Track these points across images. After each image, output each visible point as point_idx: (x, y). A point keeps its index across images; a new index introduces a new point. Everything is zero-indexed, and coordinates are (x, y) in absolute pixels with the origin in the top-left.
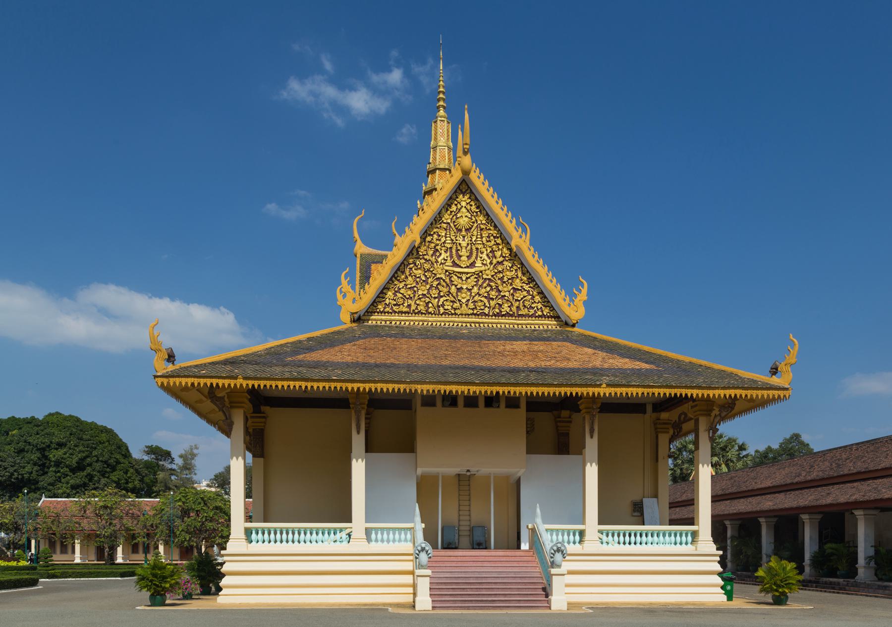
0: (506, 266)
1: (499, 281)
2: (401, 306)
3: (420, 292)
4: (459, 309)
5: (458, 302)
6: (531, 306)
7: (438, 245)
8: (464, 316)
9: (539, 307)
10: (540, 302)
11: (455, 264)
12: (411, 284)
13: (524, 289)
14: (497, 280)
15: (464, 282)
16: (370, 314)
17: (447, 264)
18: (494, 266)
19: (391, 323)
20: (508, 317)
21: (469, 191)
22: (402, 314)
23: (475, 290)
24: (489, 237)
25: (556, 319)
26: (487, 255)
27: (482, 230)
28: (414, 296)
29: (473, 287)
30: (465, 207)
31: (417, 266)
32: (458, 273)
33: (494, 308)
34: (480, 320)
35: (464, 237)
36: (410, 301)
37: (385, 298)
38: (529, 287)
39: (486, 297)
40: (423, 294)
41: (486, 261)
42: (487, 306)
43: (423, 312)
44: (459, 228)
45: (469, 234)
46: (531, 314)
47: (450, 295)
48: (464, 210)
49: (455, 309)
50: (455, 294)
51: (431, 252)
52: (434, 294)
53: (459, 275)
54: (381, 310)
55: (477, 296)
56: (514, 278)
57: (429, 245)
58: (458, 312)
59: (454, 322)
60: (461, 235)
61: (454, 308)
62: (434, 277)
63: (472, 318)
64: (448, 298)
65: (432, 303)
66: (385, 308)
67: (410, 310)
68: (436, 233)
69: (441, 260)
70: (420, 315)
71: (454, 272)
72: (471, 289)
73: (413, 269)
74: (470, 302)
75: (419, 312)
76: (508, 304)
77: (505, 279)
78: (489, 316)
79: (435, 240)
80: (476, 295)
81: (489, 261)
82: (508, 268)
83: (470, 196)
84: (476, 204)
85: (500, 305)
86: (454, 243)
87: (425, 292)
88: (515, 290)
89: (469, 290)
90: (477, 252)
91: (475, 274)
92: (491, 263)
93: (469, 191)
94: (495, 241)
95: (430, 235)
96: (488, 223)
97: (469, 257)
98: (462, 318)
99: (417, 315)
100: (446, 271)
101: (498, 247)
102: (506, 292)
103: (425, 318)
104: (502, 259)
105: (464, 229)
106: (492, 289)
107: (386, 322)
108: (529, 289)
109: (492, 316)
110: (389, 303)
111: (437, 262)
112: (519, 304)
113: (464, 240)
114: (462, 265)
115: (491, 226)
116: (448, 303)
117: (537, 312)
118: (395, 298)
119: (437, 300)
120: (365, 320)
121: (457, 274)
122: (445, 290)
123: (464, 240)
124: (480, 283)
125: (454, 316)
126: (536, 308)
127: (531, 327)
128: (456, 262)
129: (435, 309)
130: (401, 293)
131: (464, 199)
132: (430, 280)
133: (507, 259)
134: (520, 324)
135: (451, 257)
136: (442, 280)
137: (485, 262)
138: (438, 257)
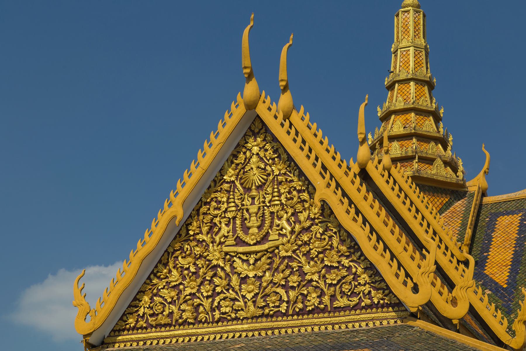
0: (316, 233)
1: (304, 258)
2: (160, 316)
3: (188, 291)
4: (242, 310)
5: (241, 300)
6: (353, 293)
7: (216, 217)
8: (250, 321)
9: (366, 292)
10: (368, 283)
11: (239, 242)
12: (176, 281)
13: (343, 265)
14: (301, 256)
15: (251, 267)
16: (117, 333)
17: (227, 243)
18: (297, 237)
19: (145, 344)
20: (318, 313)
21: (263, 131)
22: (161, 328)
25: (396, 308)
26: (288, 220)
27: (280, 183)
28: (178, 299)
30: (258, 154)
31: (185, 253)
32: (243, 254)
33: (295, 302)
34: (275, 324)
35: (253, 199)
36: (173, 307)
37: (138, 306)
38: (350, 261)
39: (283, 286)
40: (190, 294)
41: (286, 229)
42: (284, 301)
43: (190, 321)
44: (247, 187)
45: (261, 193)
47: (230, 291)
48: (255, 159)
49: (237, 311)
50: (237, 288)
51: (205, 229)
52: (207, 292)
54: (132, 325)
55: (270, 286)
56: (327, 249)
57: (204, 219)
59: (235, 331)
60: (250, 197)
61: (235, 310)
62: (208, 266)
63: (262, 322)
64: (228, 294)
65: (202, 305)
66: (137, 321)
67: (172, 321)
68: (215, 199)
69: (220, 238)
70: (186, 327)
72: (261, 277)
73: (180, 258)
74: (260, 296)
75: (185, 321)
76: (316, 293)
77: (314, 253)
78: (288, 316)
80: (268, 285)
81: (289, 228)
82: (318, 235)
83: (266, 137)
84: (273, 147)
85: (305, 296)
86: (239, 210)
87: (194, 291)
89: (260, 278)
90: (273, 219)
91: (268, 252)
92: (292, 232)
93: (263, 131)
95: (206, 203)
96: (290, 172)
97: (260, 228)
98: (247, 323)
99: (182, 327)
100: (227, 254)
101: (304, 206)
103: (194, 331)
104: (308, 223)
105: (254, 187)
106: (292, 273)
107: (138, 343)
108: (351, 264)
109: (292, 315)
110: (144, 314)
112: (335, 291)
113: (253, 204)
115: (294, 175)
116: (227, 303)
117: (363, 301)
118: (151, 305)
120: (109, 344)
121: (241, 256)
122: (224, 282)
123: (253, 204)
124: (275, 266)
125: (235, 322)
126: (361, 294)
127: (360, 326)
128: (241, 237)
129: (208, 314)
130: (161, 297)
131: (255, 143)
133: (316, 221)
134: (337, 324)
135: (234, 231)
136: (219, 269)
138: (216, 235)
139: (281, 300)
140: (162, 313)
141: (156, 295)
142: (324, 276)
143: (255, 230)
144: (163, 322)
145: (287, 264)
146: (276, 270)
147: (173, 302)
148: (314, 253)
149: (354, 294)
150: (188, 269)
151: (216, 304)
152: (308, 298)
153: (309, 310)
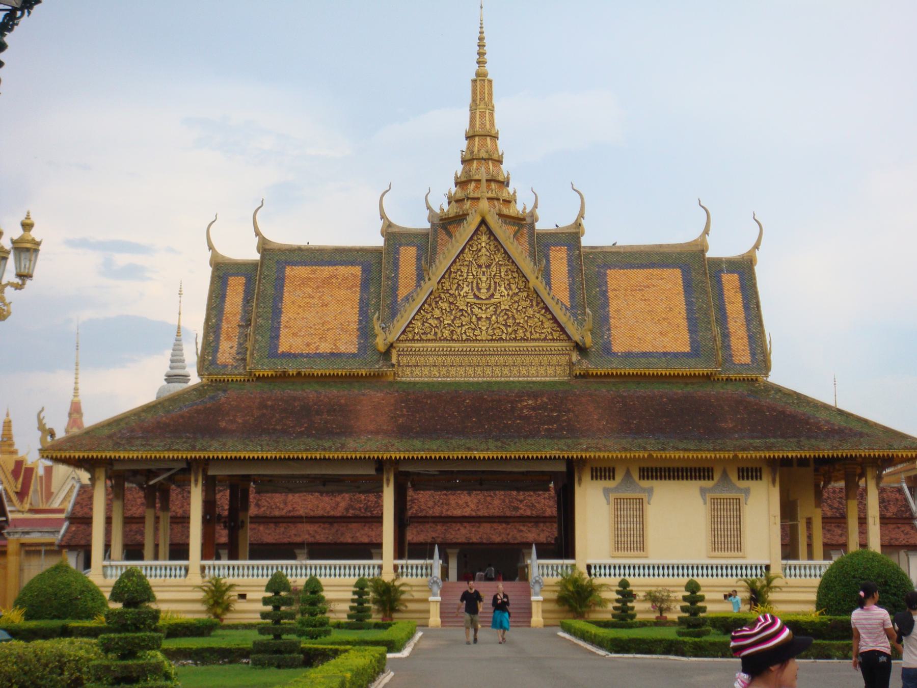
2: (429, 335)
3: (446, 322)
17: (468, 297)
24: (507, 272)
26: (505, 288)
27: (501, 265)
28: (440, 325)
29: (491, 316)
32: (478, 304)
33: (511, 334)
40: (448, 324)
46: (542, 338)
48: (484, 250)
49: (476, 336)
51: (455, 287)
53: (479, 306)
58: (479, 338)
66: (414, 336)
71: (475, 304)
73: (440, 303)
74: (490, 329)
79: (458, 276)
80: (495, 323)
81: (506, 293)
82: (524, 298)
84: (494, 244)
85: (516, 331)
87: (450, 322)
88: (529, 317)
92: (508, 295)
93: (488, 232)
94: (512, 275)
97: (489, 289)
100: (468, 303)
104: (517, 290)
105: (484, 266)
106: (508, 318)
111: (460, 295)
113: (484, 274)
114: (482, 297)
119: (460, 329)
124: (498, 313)
125: (475, 342)
132: (454, 312)
135: (472, 290)
137: (503, 294)
138: (461, 290)
139: (503, 332)
140: (430, 333)
141: (426, 322)
142: (527, 321)
143: (486, 291)
146: (499, 315)
147: (437, 327)
148: (520, 308)
150: (446, 310)
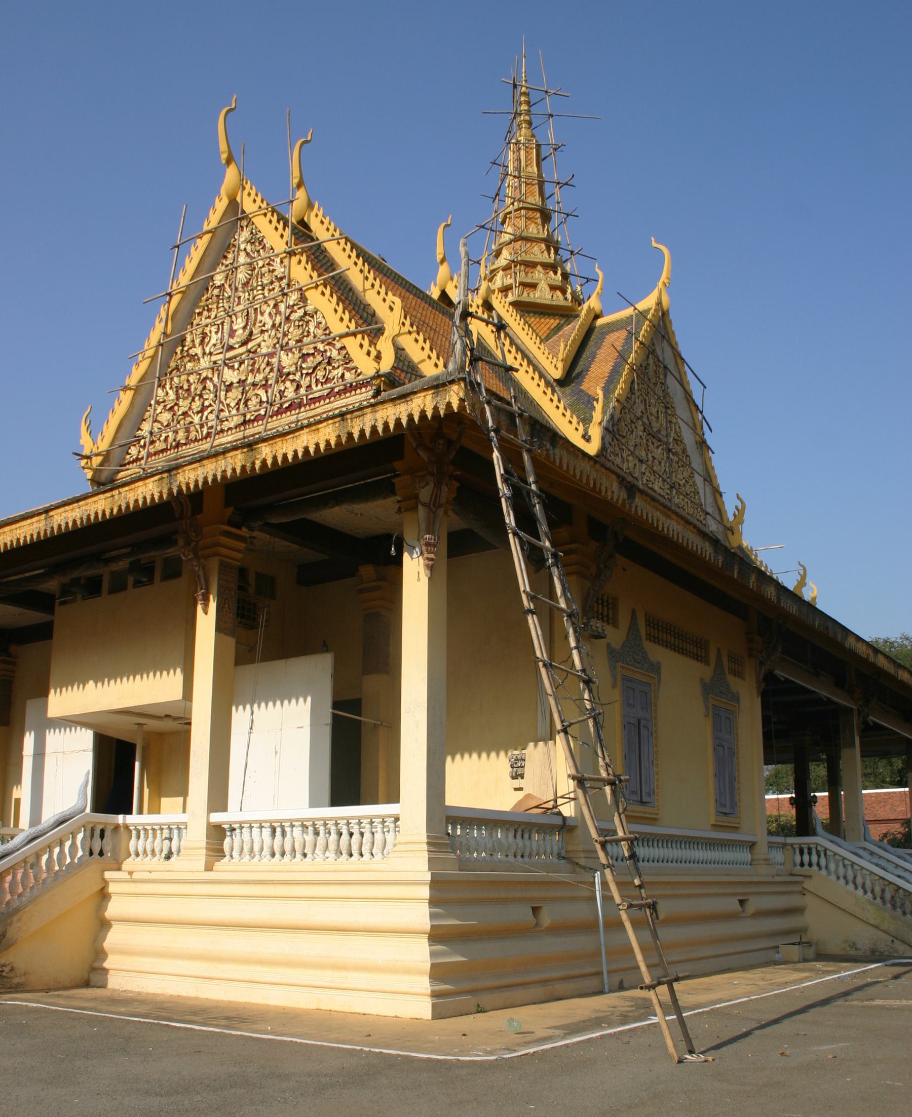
8: (234, 431)
9: (340, 375)
23: (250, 380)
42: (264, 402)
51: (197, 341)
92: (274, 326)
97: (245, 328)
100: (215, 363)
102: (291, 366)
124: (257, 366)
133: (296, 308)
139: (261, 402)
144: (160, 448)
145: (268, 361)
149: (328, 380)
151: (204, 418)
152: (286, 394)
153: (286, 408)
